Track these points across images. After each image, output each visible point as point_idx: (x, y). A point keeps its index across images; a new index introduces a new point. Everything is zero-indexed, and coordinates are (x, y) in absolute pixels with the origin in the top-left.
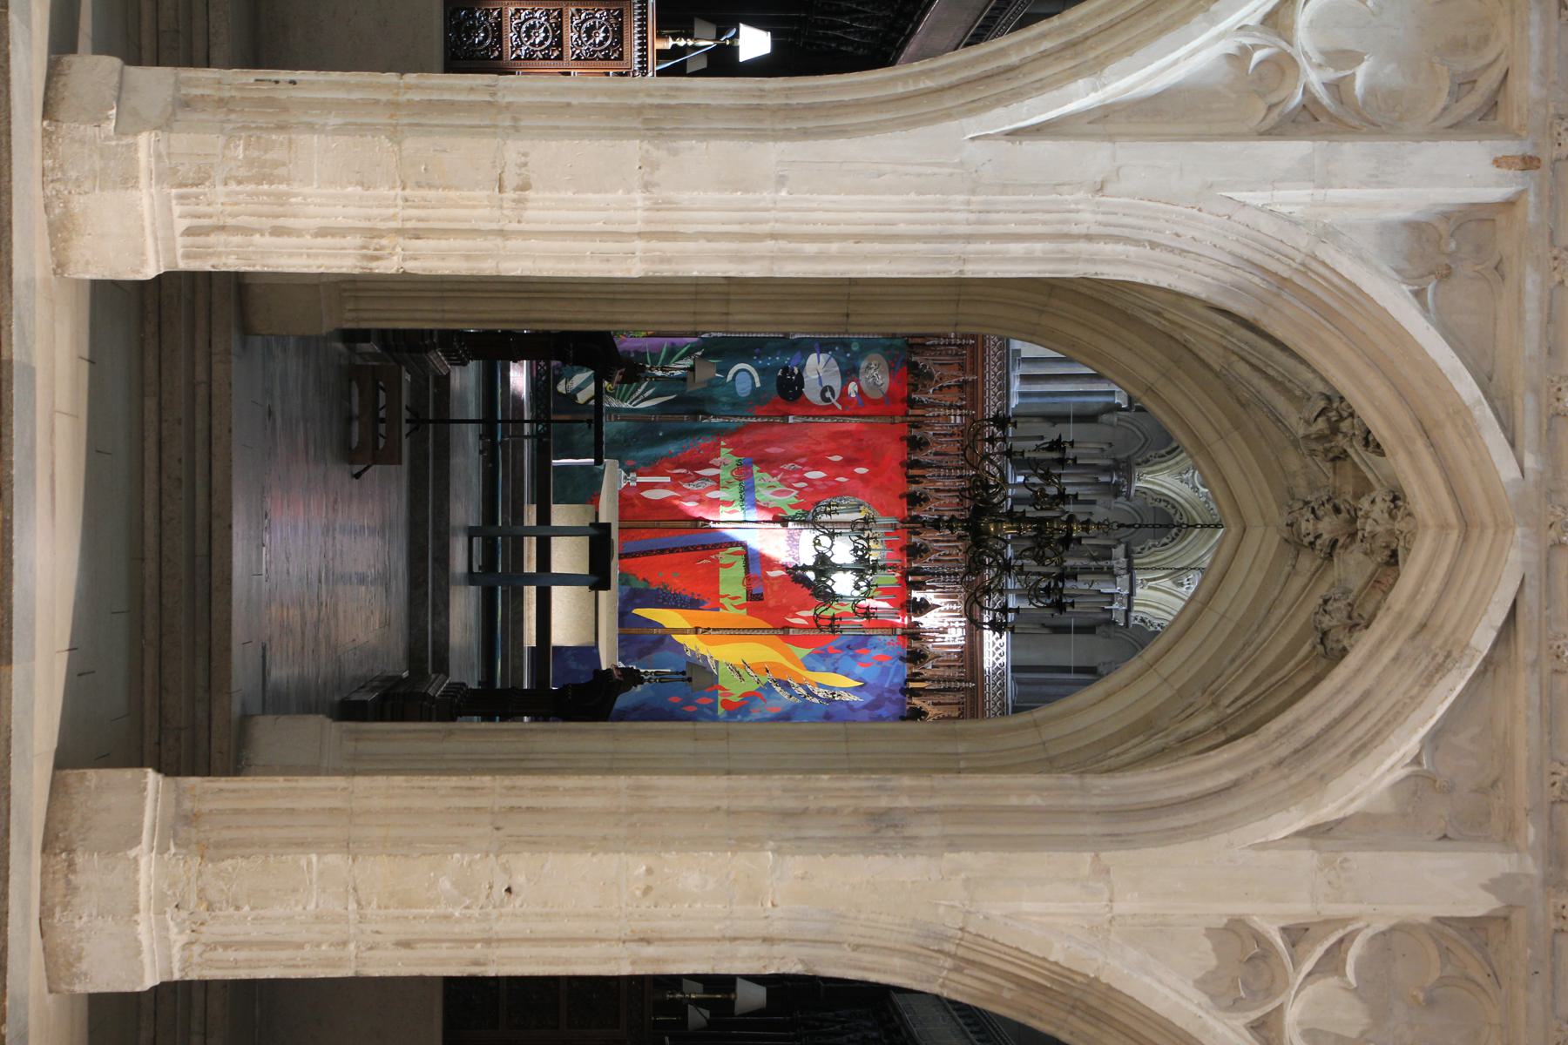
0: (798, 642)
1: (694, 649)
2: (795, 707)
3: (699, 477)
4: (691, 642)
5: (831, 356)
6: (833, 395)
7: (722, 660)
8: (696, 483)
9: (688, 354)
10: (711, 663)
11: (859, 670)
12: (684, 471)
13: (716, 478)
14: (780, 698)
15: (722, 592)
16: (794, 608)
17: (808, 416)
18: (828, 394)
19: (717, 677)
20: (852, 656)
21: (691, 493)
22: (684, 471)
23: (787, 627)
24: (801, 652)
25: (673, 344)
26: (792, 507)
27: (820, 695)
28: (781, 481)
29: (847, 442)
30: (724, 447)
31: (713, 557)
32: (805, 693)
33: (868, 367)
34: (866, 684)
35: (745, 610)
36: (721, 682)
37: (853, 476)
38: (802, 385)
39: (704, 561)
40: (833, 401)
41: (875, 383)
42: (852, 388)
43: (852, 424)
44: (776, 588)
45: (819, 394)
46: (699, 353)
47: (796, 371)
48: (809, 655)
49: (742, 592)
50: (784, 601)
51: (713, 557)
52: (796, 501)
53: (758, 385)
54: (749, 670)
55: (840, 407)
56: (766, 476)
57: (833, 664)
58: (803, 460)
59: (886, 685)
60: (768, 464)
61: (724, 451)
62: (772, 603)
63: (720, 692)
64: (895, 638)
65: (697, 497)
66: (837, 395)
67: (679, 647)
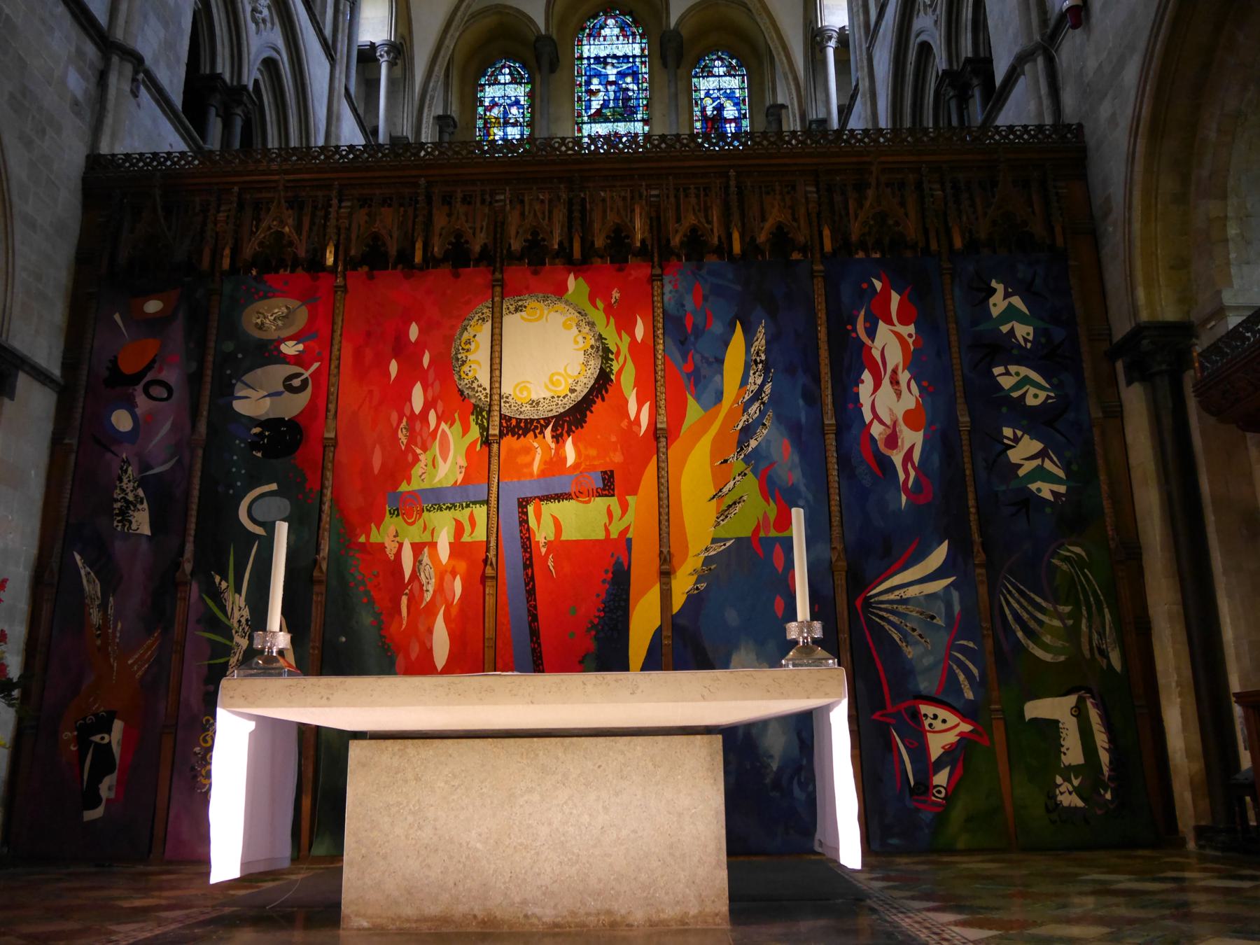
0: (678, 415)
1: (695, 577)
2: (779, 418)
3: (415, 575)
4: (683, 584)
5: (239, 379)
6: (299, 375)
7: (711, 532)
8: (424, 580)
9: (217, 596)
10: (719, 548)
11: (717, 328)
12: (404, 600)
13: (417, 548)
14: (768, 441)
15: (601, 535)
16: (624, 424)
17: (327, 410)
18: (296, 382)
19: (738, 540)
20: (697, 337)
21: (440, 589)
22: (404, 600)
23: (654, 431)
24: (694, 410)
25: (198, 621)
26: (466, 430)
27: (759, 381)
28: (425, 449)
29: (369, 354)
30: (368, 537)
31: (543, 550)
32: (757, 404)
33: (261, 327)
34: (737, 317)
35: (629, 498)
36: (746, 532)
37: (420, 346)
38: (280, 421)
39: (551, 564)
40: (306, 374)
41: (286, 317)
42: (290, 348)
43: (344, 351)
44: (593, 452)
45: (296, 396)
46: (217, 579)
47: (256, 430)
48: (697, 399)
49: (600, 503)
50: (614, 439)
51: (543, 550)
52: (458, 424)
53: (274, 487)
54: (725, 490)
55: (316, 365)
56: (416, 471)
57: (709, 364)
58: (394, 416)
59: (738, 288)
60: (401, 465)
61: (375, 537)
62: (617, 458)
63: (762, 534)
64: (666, 279)
65: (448, 577)
66: (298, 370)
67: (694, 600)
